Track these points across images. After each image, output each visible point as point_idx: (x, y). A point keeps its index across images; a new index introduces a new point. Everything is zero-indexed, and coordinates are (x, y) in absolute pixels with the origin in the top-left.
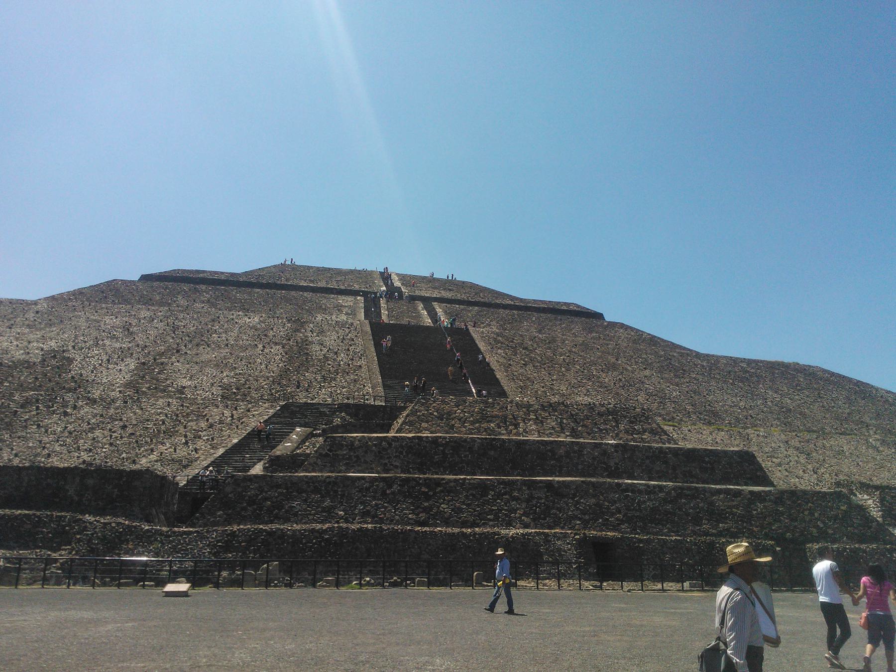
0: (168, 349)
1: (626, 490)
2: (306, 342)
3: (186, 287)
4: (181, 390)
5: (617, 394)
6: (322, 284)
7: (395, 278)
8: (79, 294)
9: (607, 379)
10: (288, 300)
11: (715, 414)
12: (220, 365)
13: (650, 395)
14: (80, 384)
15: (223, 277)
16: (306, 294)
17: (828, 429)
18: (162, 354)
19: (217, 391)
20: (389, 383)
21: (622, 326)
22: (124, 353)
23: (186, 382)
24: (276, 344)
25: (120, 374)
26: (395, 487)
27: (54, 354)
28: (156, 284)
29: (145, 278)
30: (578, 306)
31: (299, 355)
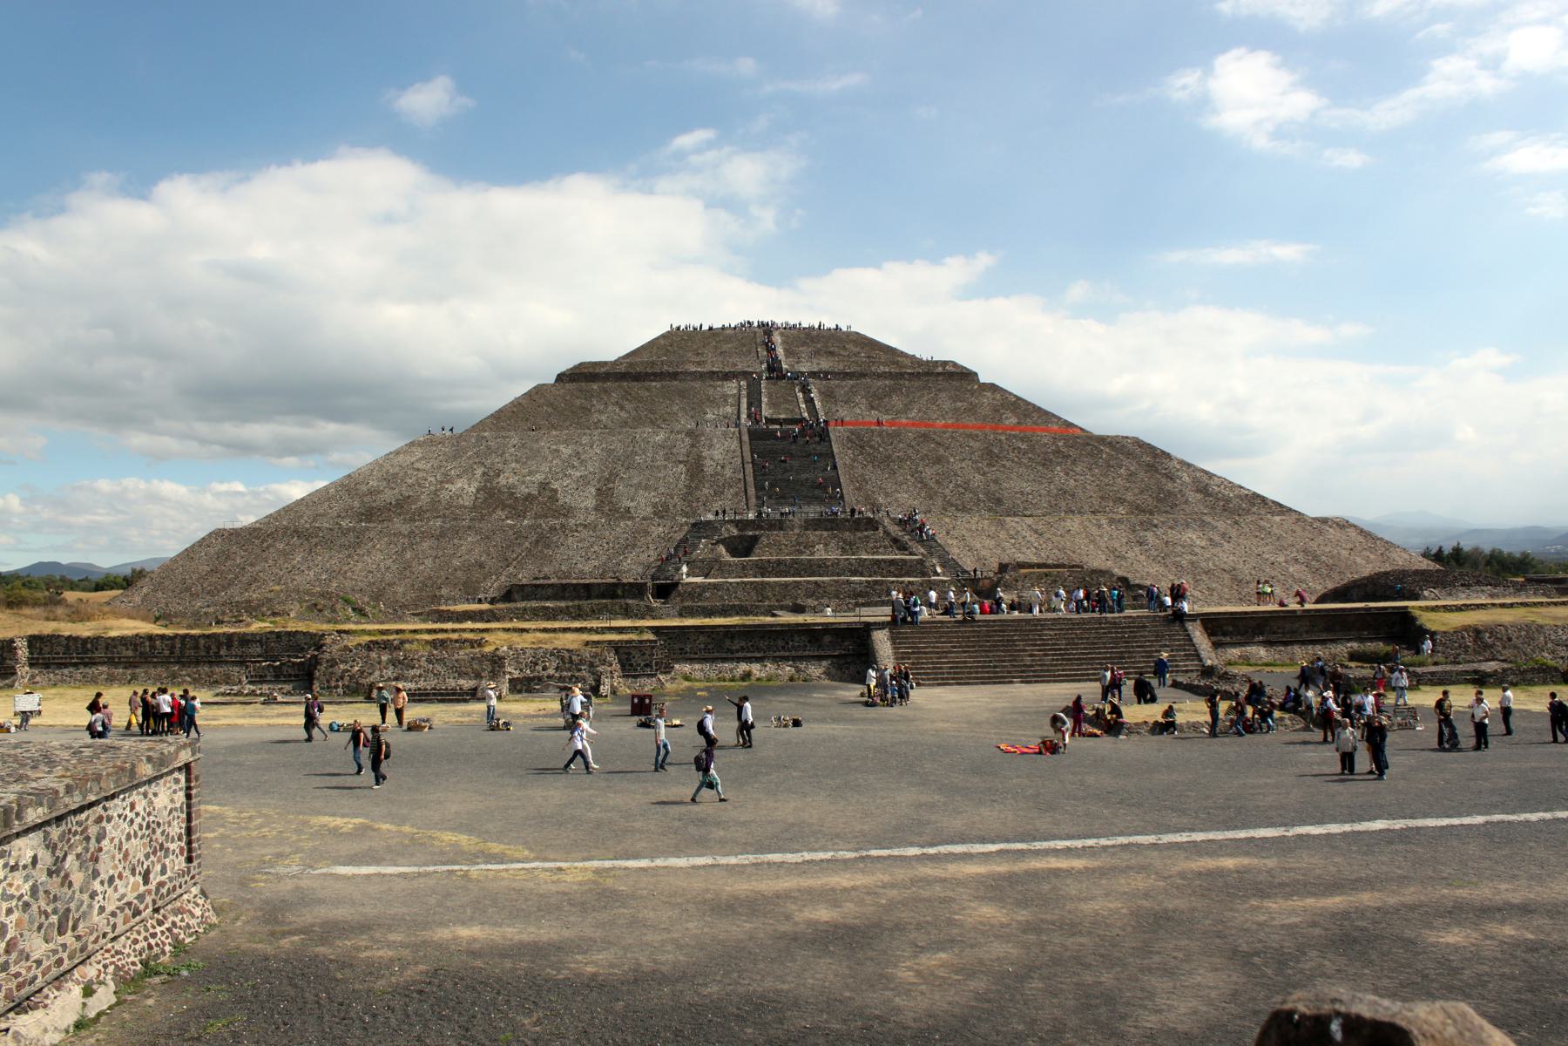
2: (700, 458)
4: (628, 510)
7: (777, 338)
9: (929, 472)
10: (682, 394)
11: (999, 501)
12: (647, 488)
13: (958, 486)
14: (568, 511)
15: (622, 369)
16: (697, 384)
17: (1086, 508)
19: (650, 509)
21: (993, 388)
22: (584, 481)
25: (586, 500)
27: (544, 486)
30: (955, 364)
31: (696, 469)
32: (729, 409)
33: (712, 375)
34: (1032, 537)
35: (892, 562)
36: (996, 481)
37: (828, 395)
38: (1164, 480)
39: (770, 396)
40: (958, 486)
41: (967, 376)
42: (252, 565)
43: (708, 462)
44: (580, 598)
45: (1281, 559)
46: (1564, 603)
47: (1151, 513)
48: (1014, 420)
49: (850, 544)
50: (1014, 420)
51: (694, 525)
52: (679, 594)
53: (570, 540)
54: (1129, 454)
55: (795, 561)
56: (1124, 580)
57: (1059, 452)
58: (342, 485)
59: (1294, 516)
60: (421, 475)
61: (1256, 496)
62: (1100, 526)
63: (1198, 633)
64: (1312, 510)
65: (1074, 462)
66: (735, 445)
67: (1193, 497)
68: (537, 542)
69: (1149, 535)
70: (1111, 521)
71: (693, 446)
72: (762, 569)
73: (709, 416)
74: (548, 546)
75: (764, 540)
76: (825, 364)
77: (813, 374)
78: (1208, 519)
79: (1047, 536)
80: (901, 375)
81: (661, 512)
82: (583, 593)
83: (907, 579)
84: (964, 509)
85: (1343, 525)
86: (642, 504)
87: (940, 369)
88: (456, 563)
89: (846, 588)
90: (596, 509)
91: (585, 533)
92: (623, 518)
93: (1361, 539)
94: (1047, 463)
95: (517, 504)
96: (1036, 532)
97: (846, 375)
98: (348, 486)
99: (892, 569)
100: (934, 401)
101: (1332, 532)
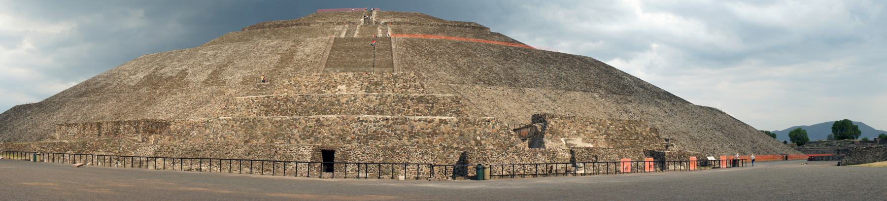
1: (362, 121)
5: (464, 70)
9: (462, 61)
11: (516, 80)
26: (238, 123)
36: (512, 69)
41: (482, 28)
43: (300, 53)
49: (376, 84)
79: (559, 102)
83: (438, 118)
84: (490, 84)
89: (355, 127)
99: (421, 107)
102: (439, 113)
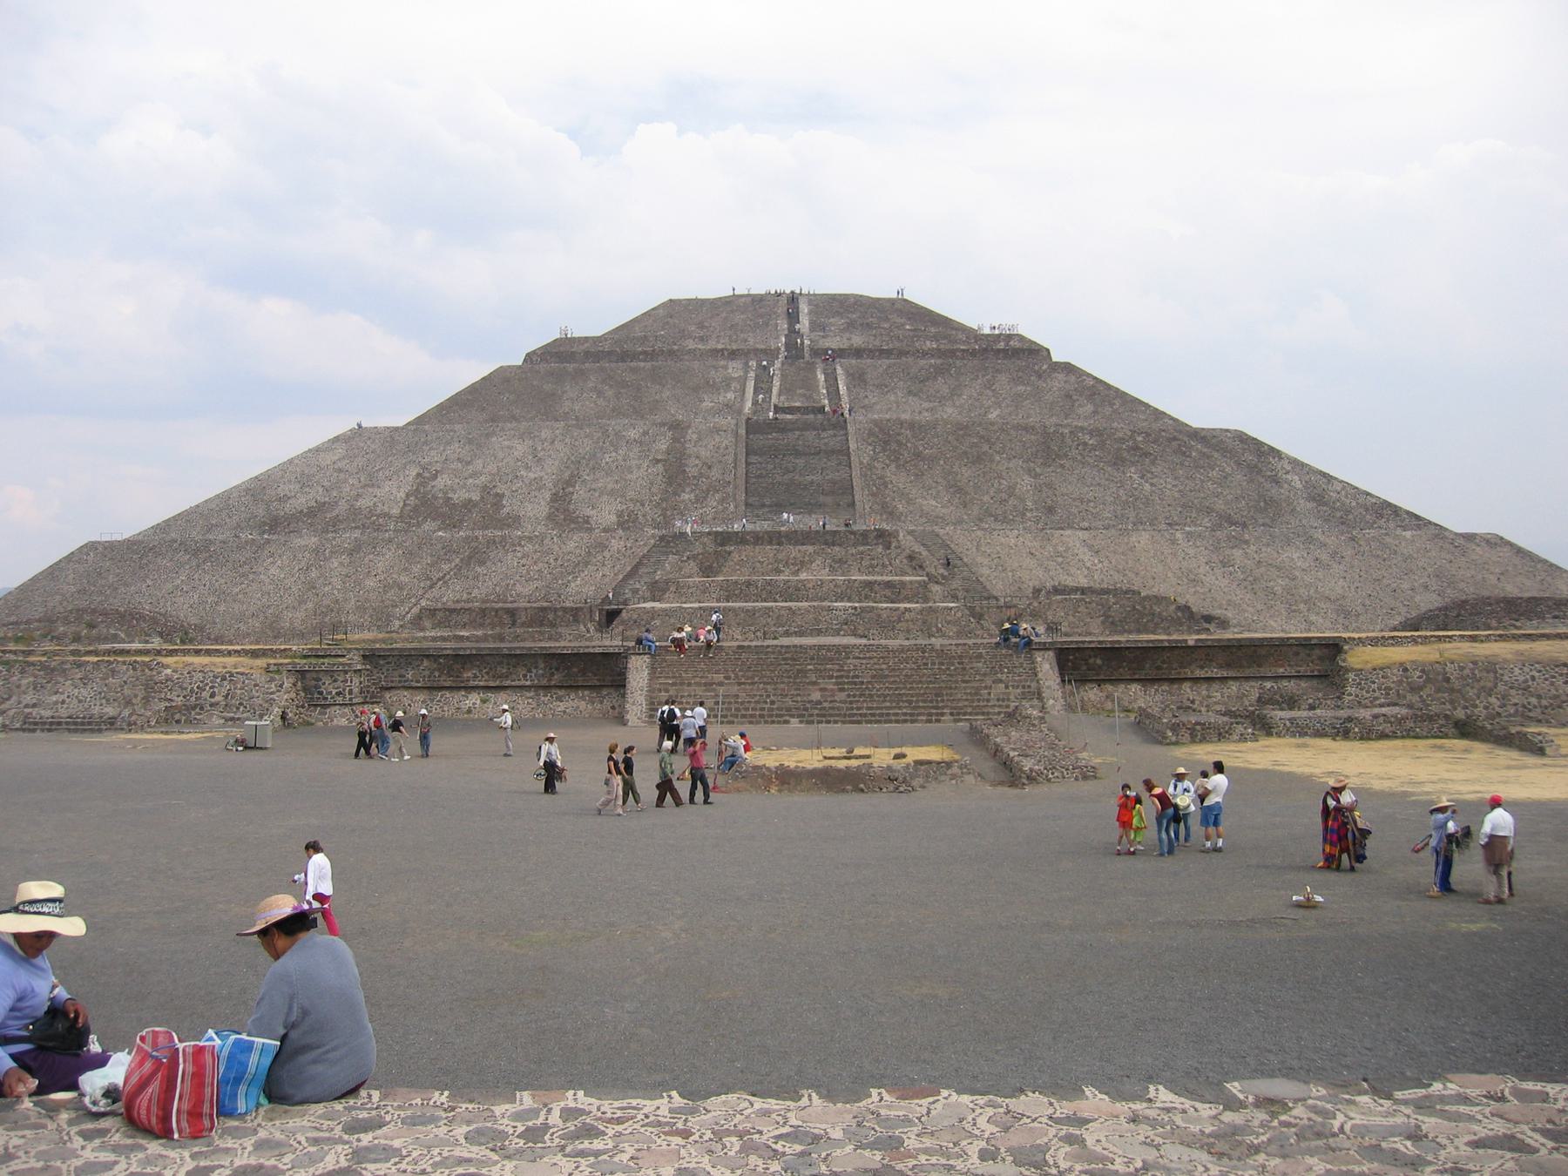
0: (572, 476)
3: (570, 367)
6: (712, 344)
7: (804, 308)
8: (473, 389)
9: (966, 473)
11: (1050, 510)
12: (612, 493)
13: (999, 491)
18: (570, 483)
19: (614, 518)
20: (750, 501)
21: (1068, 368)
22: (538, 484)
23: (589, 512)
24: (658, 461)
25: (536, 509)
28: (543, 367)
29: (529, 357)
30: (1021, 338)
32: (730, 395)
33: (715, 353)
34: (1087, 556)
35: (888, 585)
37: (857, 379)
38: (1267, 485)
39: (784, 377)
40: (999, 491)
42: (126, 585)
44: (502, 624)
45: (1405, 586)
46: (1559, 636)
47: (1244, 525)
48: (1090, 408)
50: (1090, 408)
51: (662, 538)
52: (623, 622)
53: (510, 556)
54: (1226, 451)
55: (769, 583)
56: (1186, 609)
57: (1136, 448)
58: (247, 490)
59: (1433, 531)
60: (342, 476)
61: (1389, 505)
62: (1174, 542)
63: (1047, 666)
64: (1457, 523)
65: (1153, 463)
66: (727, 440)
67: (1304, 505)
68: (470, 557)
69: (1237, 553)
70: (1189, 535)
71: (675, 440)
72: (730, 591)
73: (707, 404)
74: (482, 563)
75: (736, 556)
76: (857, 340)
77: (840, 353)
78: (1318, 535)
80: (952, 353)
81: (627, 522)
82: (506, 619)
83: (902, 606)
85: (1495, 542)
86: (606, 515)
87: (1002, 345)
88: (370, 583)
90: (550, 517)
91: (529, 548)
92: (580, 529)
93: (1517, 560)
94: (1118, 462)
95: (450, 513)
96: (1091, 547)
97: (883, 353)
98: (257, 489)
100: (989, 385)
101: (1479, 551)
102: (908, 599)
